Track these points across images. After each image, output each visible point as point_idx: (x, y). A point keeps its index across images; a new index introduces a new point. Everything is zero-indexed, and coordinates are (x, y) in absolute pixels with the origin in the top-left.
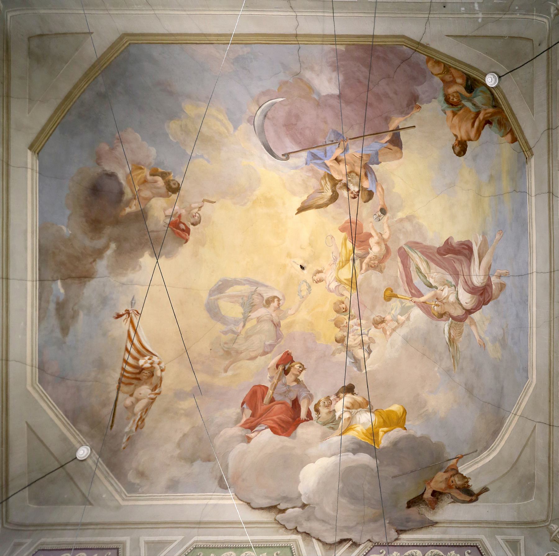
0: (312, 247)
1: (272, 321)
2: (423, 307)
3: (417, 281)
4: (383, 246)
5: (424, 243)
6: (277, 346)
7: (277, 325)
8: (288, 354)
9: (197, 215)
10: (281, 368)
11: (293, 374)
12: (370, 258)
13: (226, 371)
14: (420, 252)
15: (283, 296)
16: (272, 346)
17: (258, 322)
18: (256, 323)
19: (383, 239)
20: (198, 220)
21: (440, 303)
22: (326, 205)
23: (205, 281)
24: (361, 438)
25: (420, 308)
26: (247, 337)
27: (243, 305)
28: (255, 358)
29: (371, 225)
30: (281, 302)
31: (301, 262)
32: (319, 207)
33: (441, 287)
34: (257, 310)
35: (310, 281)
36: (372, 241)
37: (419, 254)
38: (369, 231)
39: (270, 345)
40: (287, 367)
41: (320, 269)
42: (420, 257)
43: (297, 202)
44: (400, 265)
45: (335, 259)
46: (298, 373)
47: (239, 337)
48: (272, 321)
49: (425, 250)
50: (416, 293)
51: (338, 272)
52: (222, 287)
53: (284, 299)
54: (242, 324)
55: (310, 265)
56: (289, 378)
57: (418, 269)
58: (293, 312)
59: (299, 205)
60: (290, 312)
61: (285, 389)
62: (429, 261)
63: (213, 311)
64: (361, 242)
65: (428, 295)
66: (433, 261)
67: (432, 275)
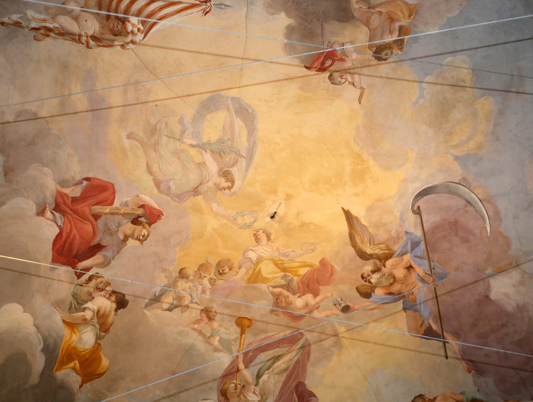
0: (300, 226)
1: (201, 184)
2: (233, 368)
3: (263, 357)
4: (302, 312)
5: (309, 365)
6: (169, 198)
7: (196, 191)
8: (159, 216)
9: (343, 80)
10: (140, 212)
11: (134, 231)
12: (288, 297)
13: (130, 136)
14: (299, 359)
15: (235, 193)
16: (168, 192)
17: (199, 164)
18: (197, 161)
19: (311, 312)
20: (336, 82)
21: (238, 390)
22: (354, 245)
23: (253, 96)
24: (63, 346)
25: (231, 364)
26: (177, 154)
27: (221, 141)
28: (151, 173)
29: (329, 294)
30: (227, 191)
31: (280, 213)
32: (352, 237)
33: (258, 390)
34: (215, 160)
35: (257, 225)
36: (309, 298)
37: (296, 358)
38: (321, 293)
39: (169, 188)
40: (142, 219)
41: (272, 237)
42: (292, 360)
43: (358, 212)
44: (281, 335)
45: (285, 255)
46: (136, 236)
47: (177, 142)
48: (201, 184)
49: (301, 365)
50: (248, 357)
51: (269, 259)
52: (245, 113)
53: (231, 195)
54: (194, 142)
55: (276, 225)
56: (128, 227)
57: (278, 358)
58: (214, 209)
59: (354, 212)
60: (214, 206)
61: (113, 227)
62: (288, 372)
63: (210, 104)
64: (308, 284)
65: (248, 374)
66: (289, 378)
67: (272, 377)
